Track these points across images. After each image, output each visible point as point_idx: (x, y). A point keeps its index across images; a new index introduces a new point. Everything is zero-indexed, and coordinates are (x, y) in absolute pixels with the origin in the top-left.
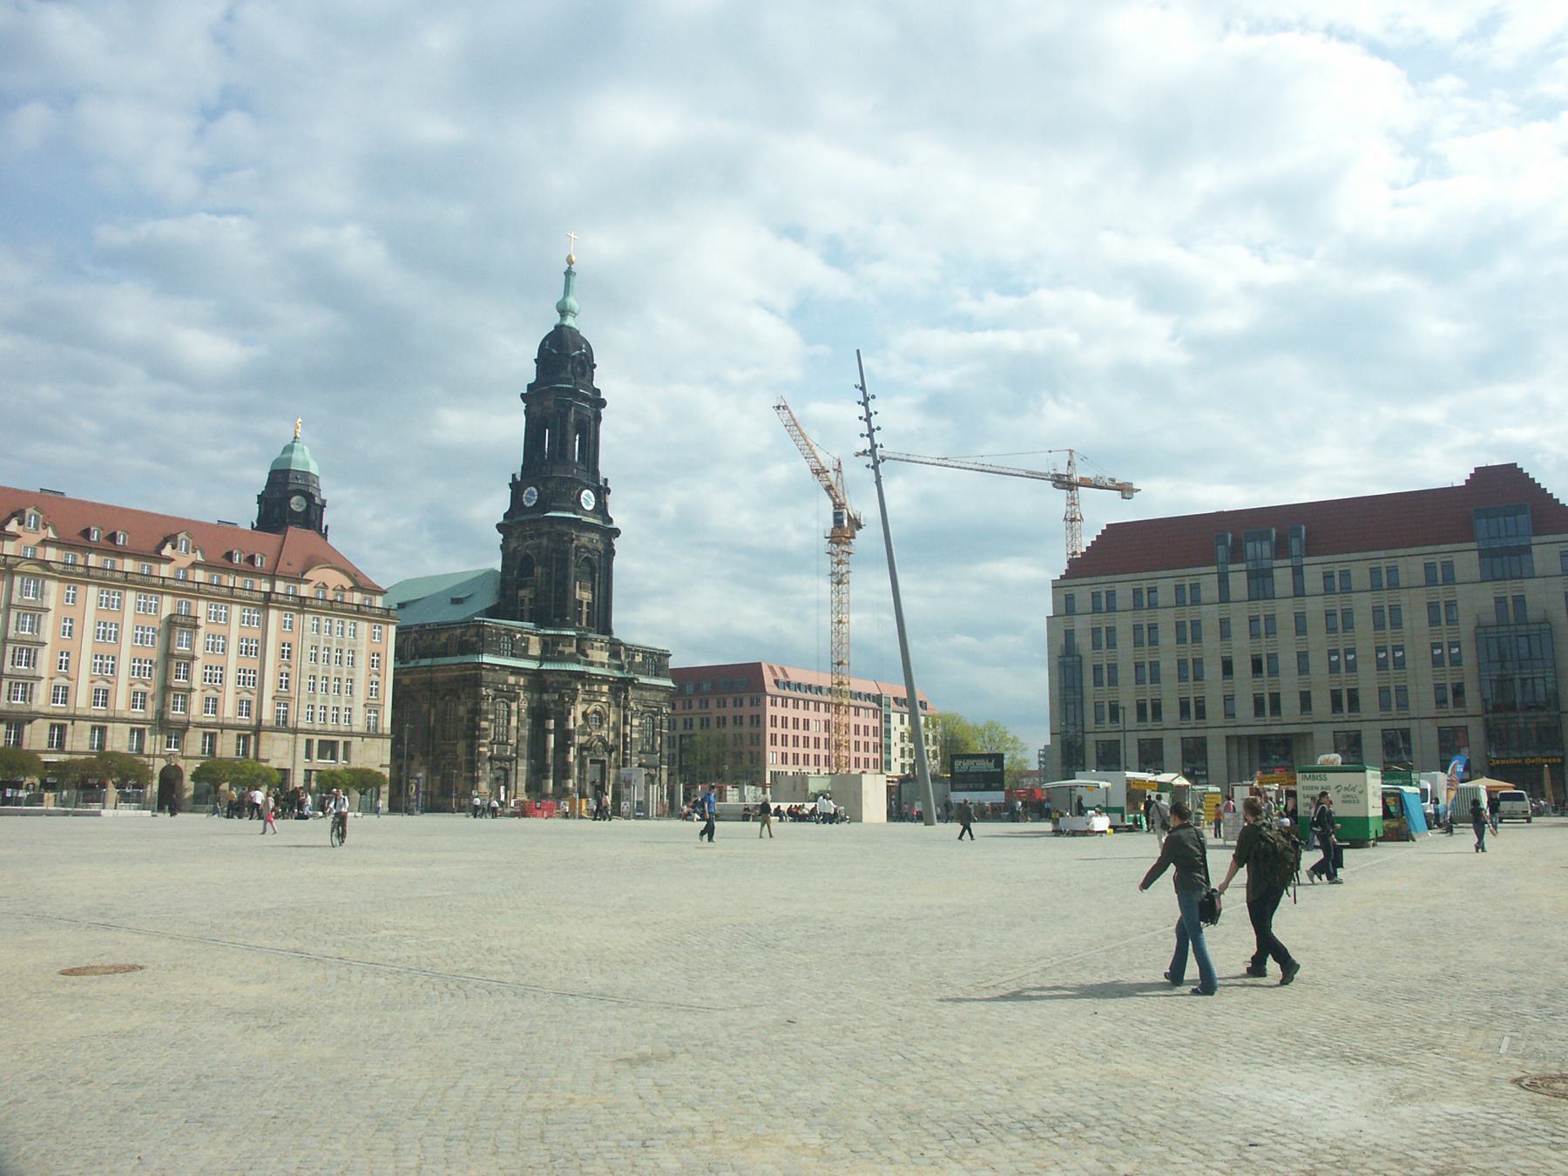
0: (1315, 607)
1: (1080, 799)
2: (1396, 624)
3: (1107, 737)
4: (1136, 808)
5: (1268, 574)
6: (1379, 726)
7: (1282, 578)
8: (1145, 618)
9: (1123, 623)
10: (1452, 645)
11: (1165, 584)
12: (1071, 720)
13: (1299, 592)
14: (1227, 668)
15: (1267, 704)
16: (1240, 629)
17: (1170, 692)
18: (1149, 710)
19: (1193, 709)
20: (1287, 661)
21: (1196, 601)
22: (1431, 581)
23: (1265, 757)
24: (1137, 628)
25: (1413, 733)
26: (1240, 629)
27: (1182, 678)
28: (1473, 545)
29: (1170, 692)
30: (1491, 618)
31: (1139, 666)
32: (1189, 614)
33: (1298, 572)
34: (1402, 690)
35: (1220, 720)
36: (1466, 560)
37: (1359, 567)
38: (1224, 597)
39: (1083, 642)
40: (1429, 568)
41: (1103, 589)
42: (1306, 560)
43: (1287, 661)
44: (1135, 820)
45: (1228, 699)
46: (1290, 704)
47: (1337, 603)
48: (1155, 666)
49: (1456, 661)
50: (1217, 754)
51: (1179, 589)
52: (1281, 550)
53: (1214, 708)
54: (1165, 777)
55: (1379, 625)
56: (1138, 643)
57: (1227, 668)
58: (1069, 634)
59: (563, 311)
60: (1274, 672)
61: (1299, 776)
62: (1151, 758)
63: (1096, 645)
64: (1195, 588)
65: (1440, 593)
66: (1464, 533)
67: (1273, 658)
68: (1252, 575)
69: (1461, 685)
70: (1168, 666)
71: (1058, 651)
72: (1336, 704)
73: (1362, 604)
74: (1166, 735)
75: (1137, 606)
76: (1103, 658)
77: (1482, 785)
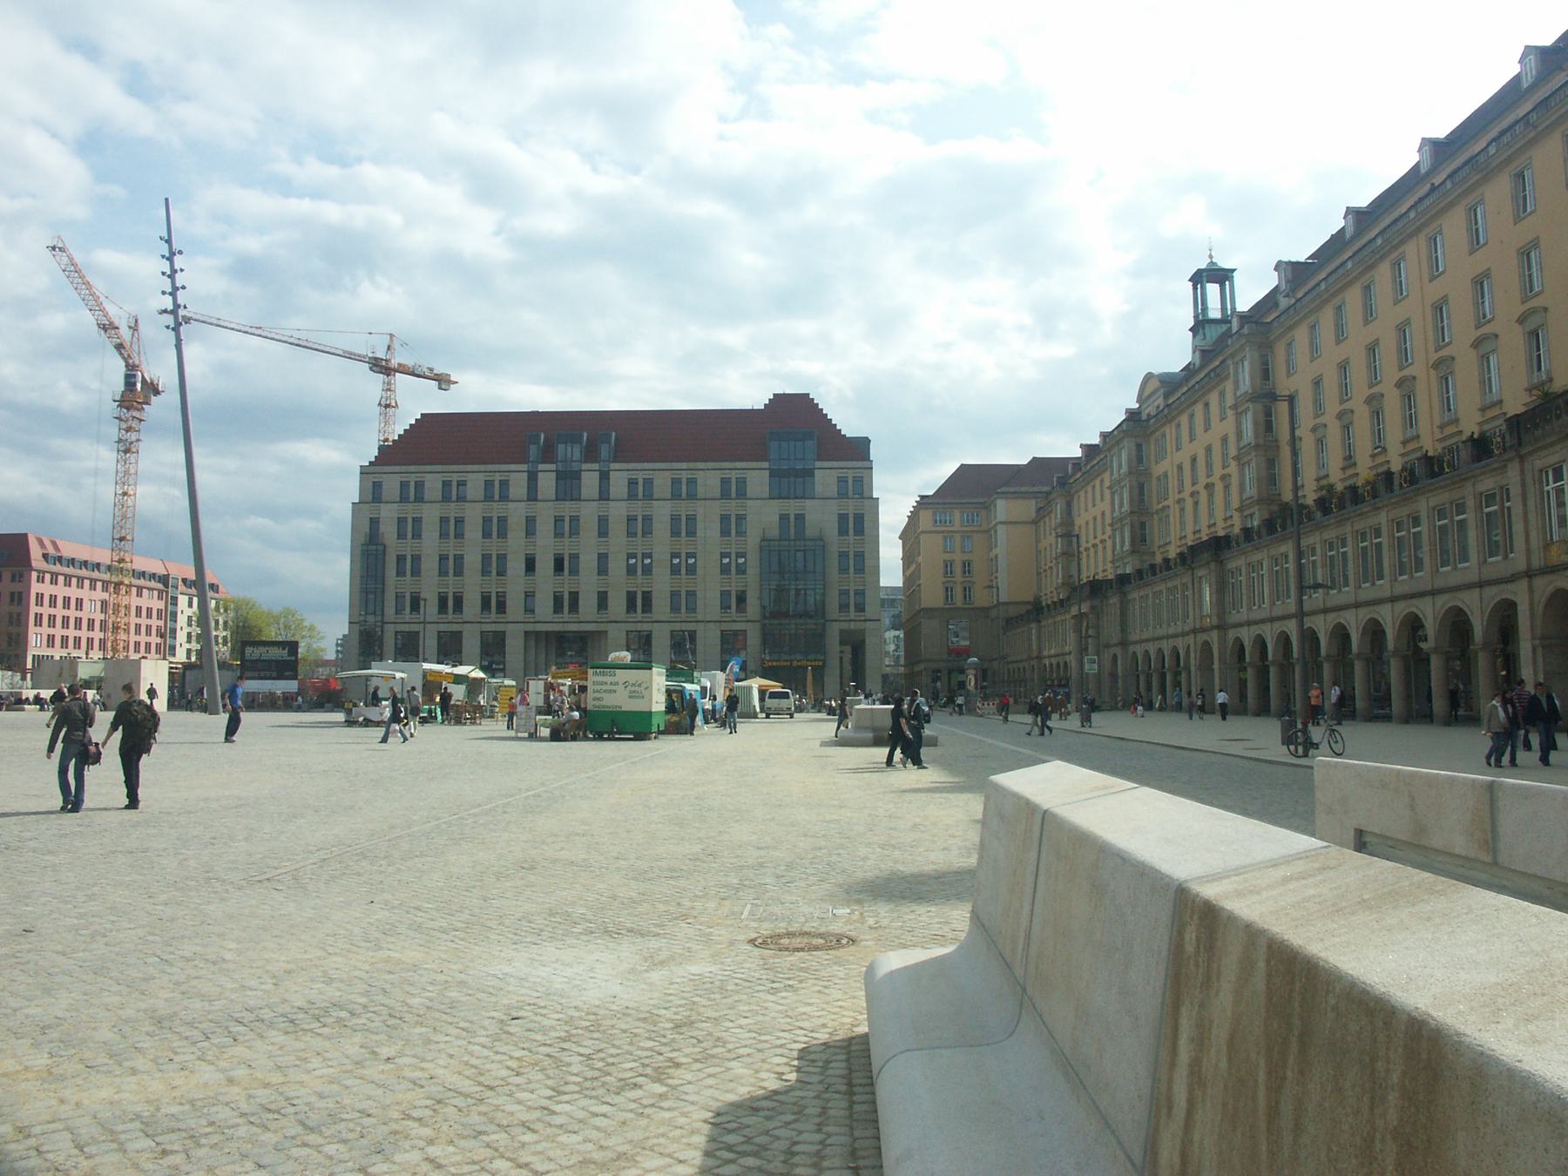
0: (618, 511)
1: (377, 689)
2: (691, 532)
3: (406, 628)
4: (432, 700)
5: (576, 475)
6: (667, 628)
7: (589, 481)
8: (452, 510)
9: (430, 514)
10: (739, 555)
11: (475, 478)
12: (371, 608)
13: (604, 496)
14: (530, 565)
15: (567, 602)
16: (545, 527)
17: (472, 586)
18: (450, 603)
19: (494, 603)
20: (588, 562)
21: (504, 497)
22: (725, 495)
23: (561, 653)
24: (444, 520)
25: (699, 635)
26: (545, 527)
27: (485, 572)
28: (766, 465)
29: (472, 586)
30: (774, 532)
31: (443, 558)
32: (496, 510)
33: (604, 476)
34: (691, 594)
35: (520, 616)
36: (758, 478)
37: (661, 476)
38: (532, 496)
39: (388, 531)
40: (725, 482)
41: (412, 479)
42: (614, 466)
43: (588, 562)
44: (430, 711)
45: (529, 595)
46: (588, 604)
47: (638, 508)
48: (459, 559)
49: (741, 570)
50: (515, 647)
51: (489, 484)
52: (591, 454)
54: (462, 670)
55: (675, 533)
56: (443, 535)
57: (530, 565)
58: (374, 522)
59: (1211, 257)
60: (574, 571)
61: (590, 671)
62: (450, 650)
63: (401, 535)
64: (504, 484)
65: (733, 507)
66: (757, 452)
67: (575, 557)
68: (560, 476)
69: (744, 592)
70: (472, 560)
71: (362, 540)
72: (631, 606)
73: (662, 512)
74: (466, 628)
75: (446, 498)
76: (408, 547)
77: (755, 684)
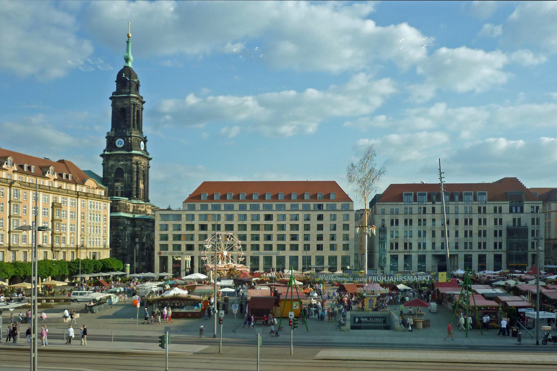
30: (511, 224)
34: (485, 244)
39: (388, 224)
53: (429, 247)
65: (498, 216)
72: (466, 248)
